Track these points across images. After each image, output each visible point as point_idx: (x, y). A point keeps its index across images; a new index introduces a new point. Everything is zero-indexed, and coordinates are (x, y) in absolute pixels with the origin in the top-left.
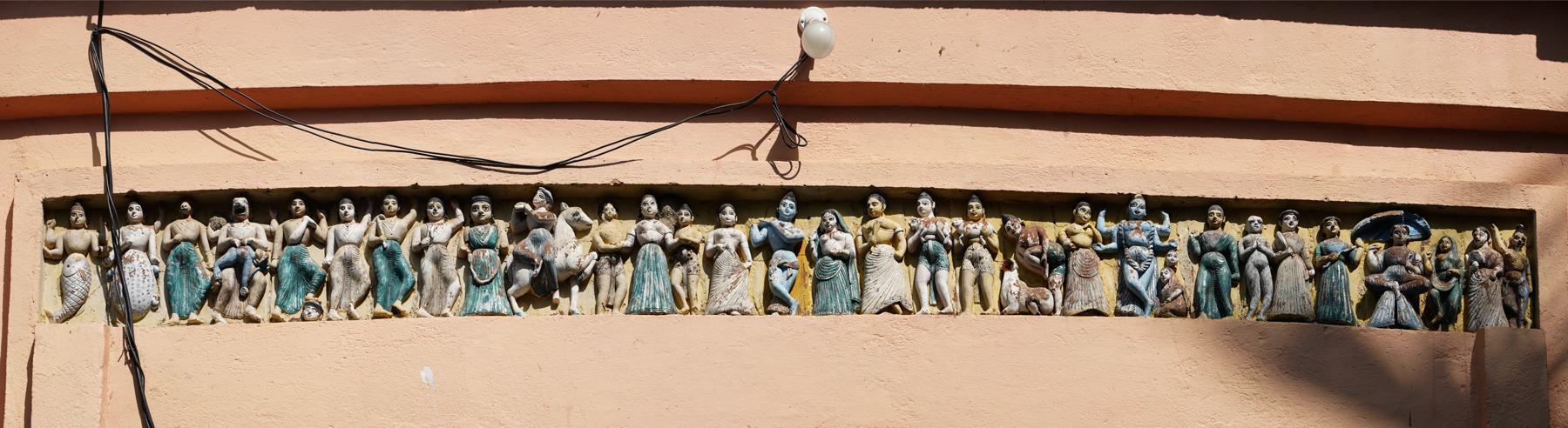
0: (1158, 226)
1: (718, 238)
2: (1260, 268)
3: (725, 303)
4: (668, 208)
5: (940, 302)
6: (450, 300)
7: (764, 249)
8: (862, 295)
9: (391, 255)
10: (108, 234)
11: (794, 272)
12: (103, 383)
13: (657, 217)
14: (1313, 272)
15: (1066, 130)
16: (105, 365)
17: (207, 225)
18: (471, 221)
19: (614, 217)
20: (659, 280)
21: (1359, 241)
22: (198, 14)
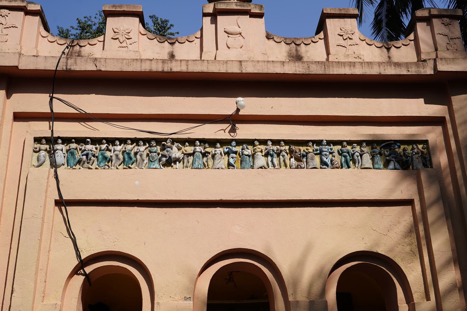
0: (330, 147)
1: (215, 151)
2: (358, 156)
3: (217, 166)
4: (202, 144)
5: (274, 166)
6: (144, 165)
7: (228, 154)
8: (253, 164)
9: (129, 154)
10: (52, 146)
11: (236, 159)
12: (47, 183)
13: (199, 146)
14: (371, 157)
15: (304, 125)
16: (48, 178)
17: (79, 145)
18: (150, 146)
19: (188, 146)
20: (200, 161)
21: (382, 149)
22: (79, 95)
